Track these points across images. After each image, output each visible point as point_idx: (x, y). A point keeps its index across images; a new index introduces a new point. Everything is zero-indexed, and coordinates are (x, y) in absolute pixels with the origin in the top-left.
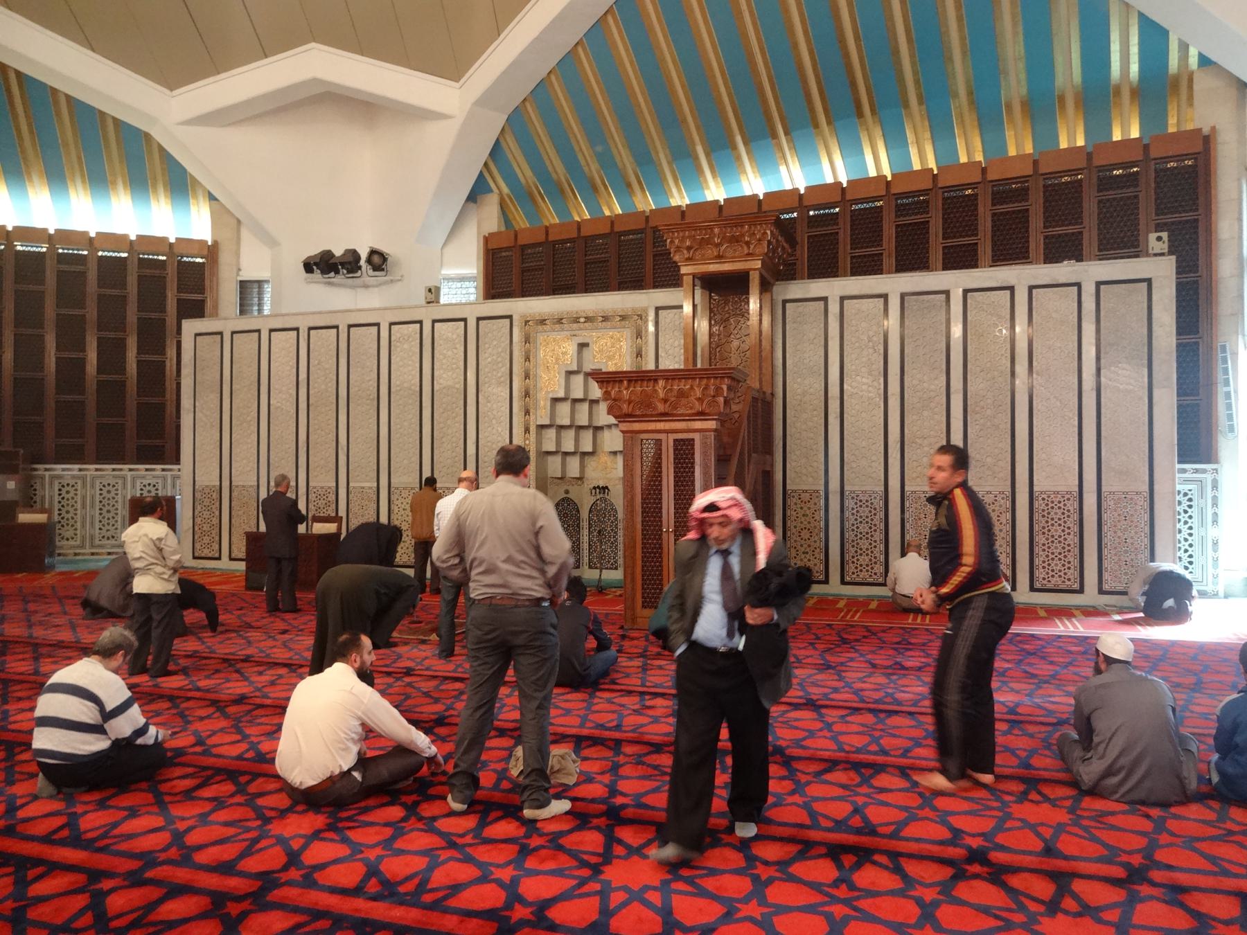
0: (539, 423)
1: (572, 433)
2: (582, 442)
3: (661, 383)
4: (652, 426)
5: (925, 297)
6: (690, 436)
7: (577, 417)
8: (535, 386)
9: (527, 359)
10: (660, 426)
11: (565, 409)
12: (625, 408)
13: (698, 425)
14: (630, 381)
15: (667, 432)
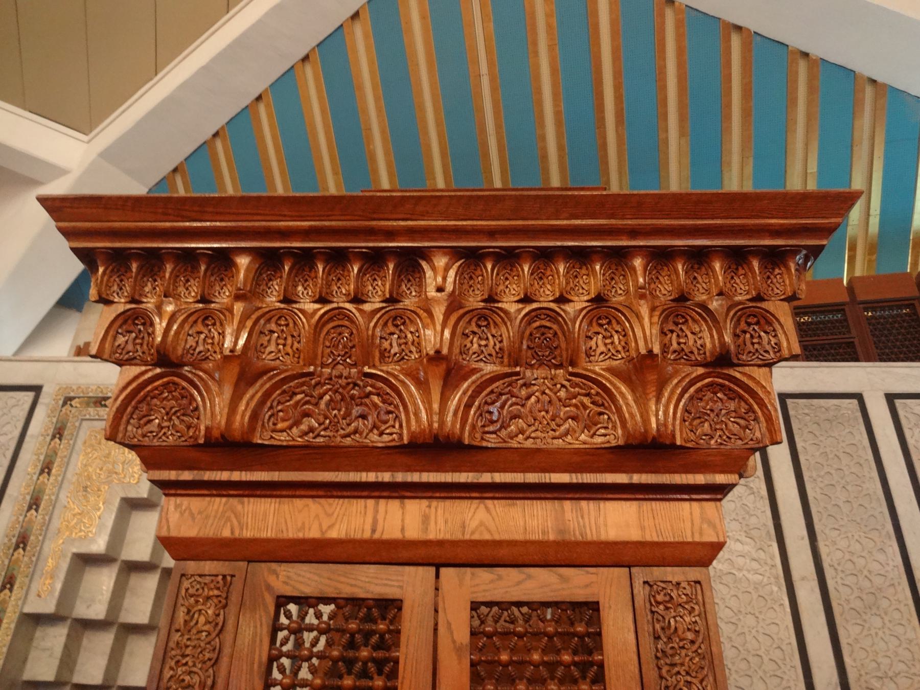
0: (28, 609)
1: (106, 640)
2: (83, 658)
3: (440, 275)
4: (350, 520)
5: (822, 402)
6: (575, 584)
7: (127, 602)
8: (46, 525)
9: (46, 468)
10: (402, 520)
11: (102, 582)
12: (217, 408)
13: (618, 521)
14: (268, 261)
15: (438, 557)
